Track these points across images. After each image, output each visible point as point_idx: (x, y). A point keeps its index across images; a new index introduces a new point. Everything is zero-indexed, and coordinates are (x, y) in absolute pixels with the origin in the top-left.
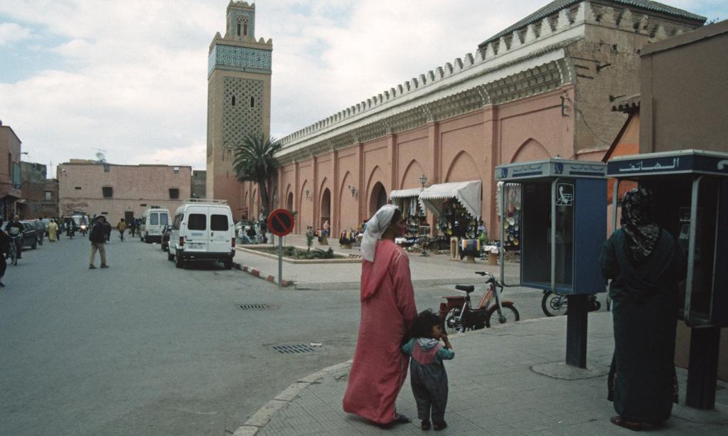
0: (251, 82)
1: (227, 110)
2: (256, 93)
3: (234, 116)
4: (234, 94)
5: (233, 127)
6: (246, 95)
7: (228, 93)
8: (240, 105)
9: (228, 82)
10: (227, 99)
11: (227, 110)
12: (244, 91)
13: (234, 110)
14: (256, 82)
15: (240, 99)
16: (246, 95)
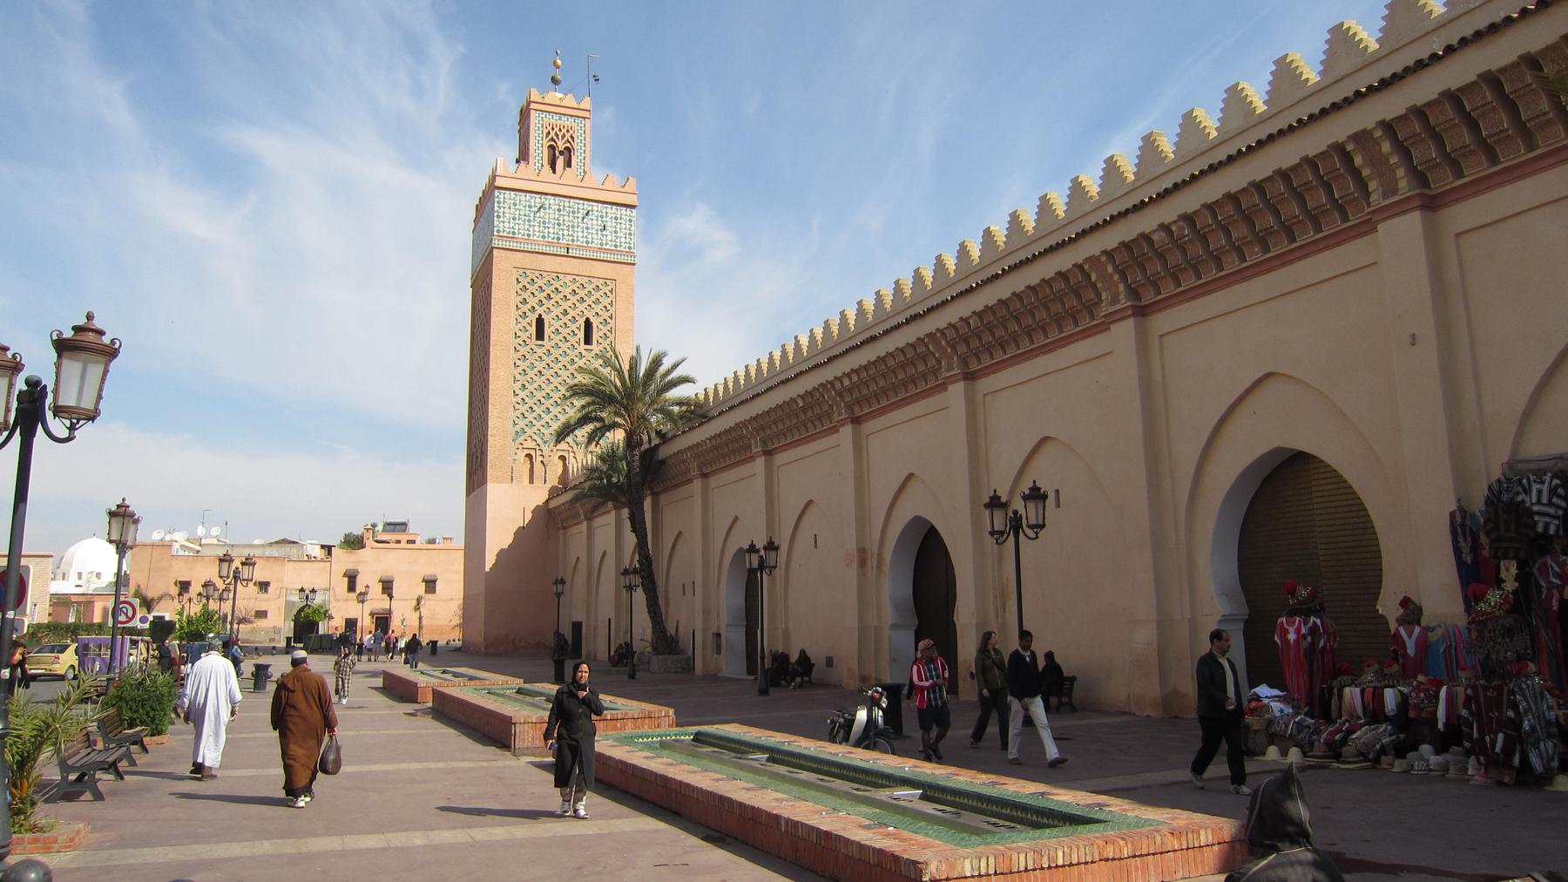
0: (584, 280)
1: (523, 350)
2: (598, 308)
3: (540, 366)
4: (540, 310)
5: (539, 395)
6: (572, 313)
7: (525, 308)
8: (557, 338)
9: (525, 281)
10: (524, 323)
11: (523, 350)
12: (565, 305)
13: (540, 351)
14: (596, 282)
15: (557, 324)
16: (572, 313)
